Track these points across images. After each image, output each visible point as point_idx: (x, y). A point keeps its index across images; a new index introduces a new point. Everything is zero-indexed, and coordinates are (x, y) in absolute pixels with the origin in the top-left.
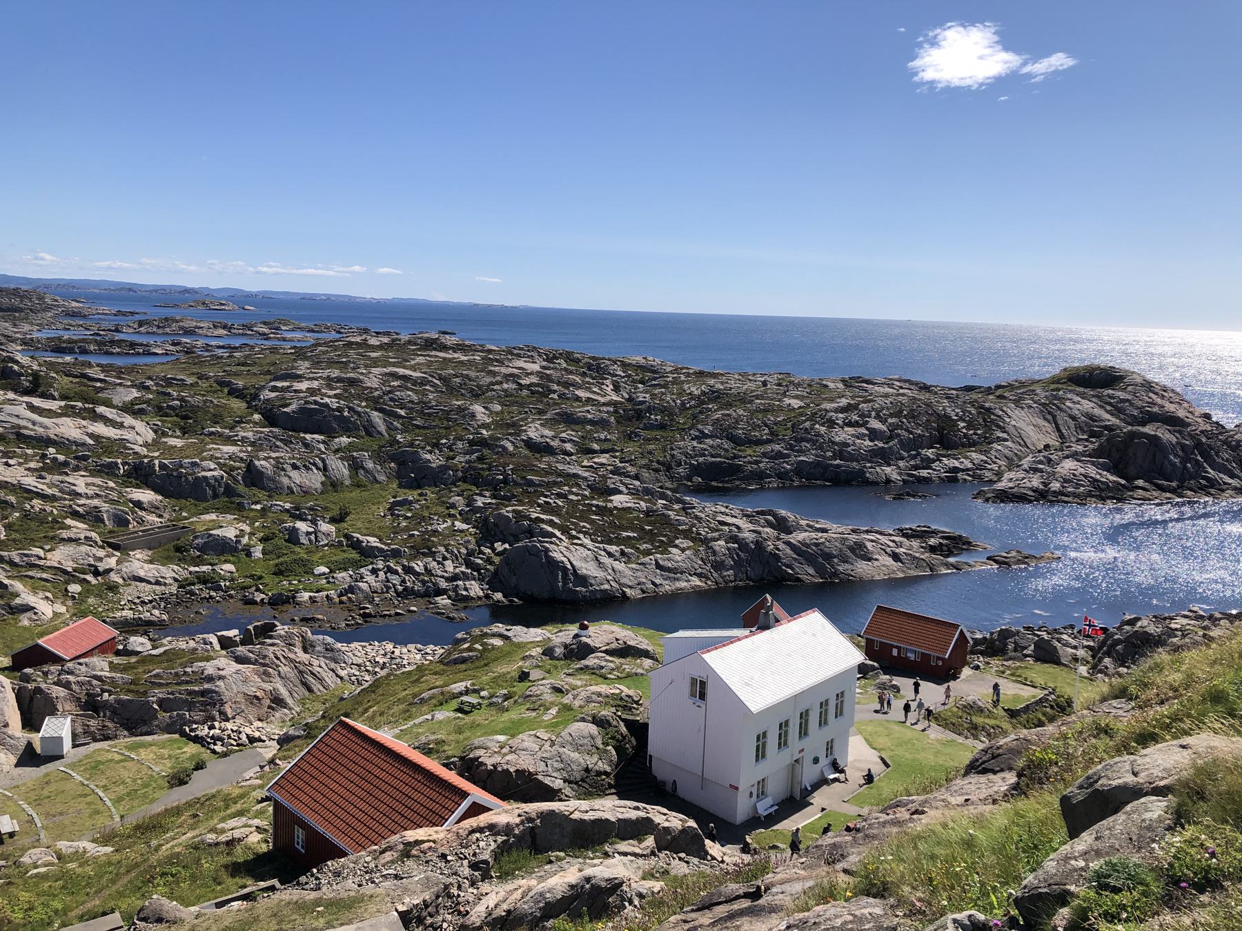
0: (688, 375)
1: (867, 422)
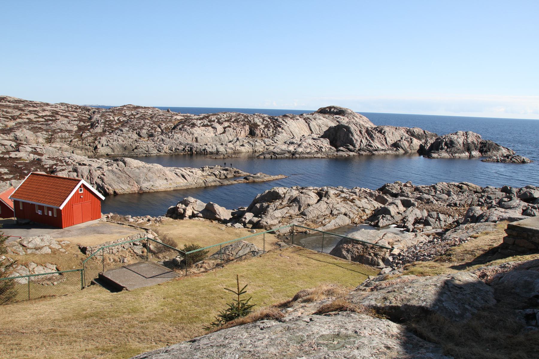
1: (212, 125)
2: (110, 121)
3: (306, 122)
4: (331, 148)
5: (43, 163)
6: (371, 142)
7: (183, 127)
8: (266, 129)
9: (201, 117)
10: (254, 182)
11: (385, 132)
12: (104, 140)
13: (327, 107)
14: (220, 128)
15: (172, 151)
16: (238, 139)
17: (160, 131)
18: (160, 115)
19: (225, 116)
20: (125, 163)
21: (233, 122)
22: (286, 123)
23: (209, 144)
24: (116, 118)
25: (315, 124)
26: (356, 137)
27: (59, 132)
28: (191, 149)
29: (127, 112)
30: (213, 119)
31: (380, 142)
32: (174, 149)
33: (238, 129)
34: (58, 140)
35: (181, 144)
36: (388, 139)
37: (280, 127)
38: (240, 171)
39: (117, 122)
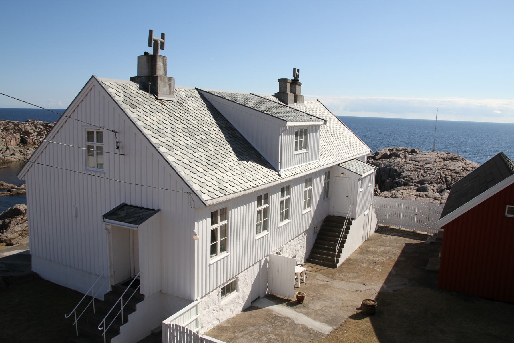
8: (39, 137)
10: (18, 194)
16: (7, 148)
33: (8, 138)
38: (5, 183)
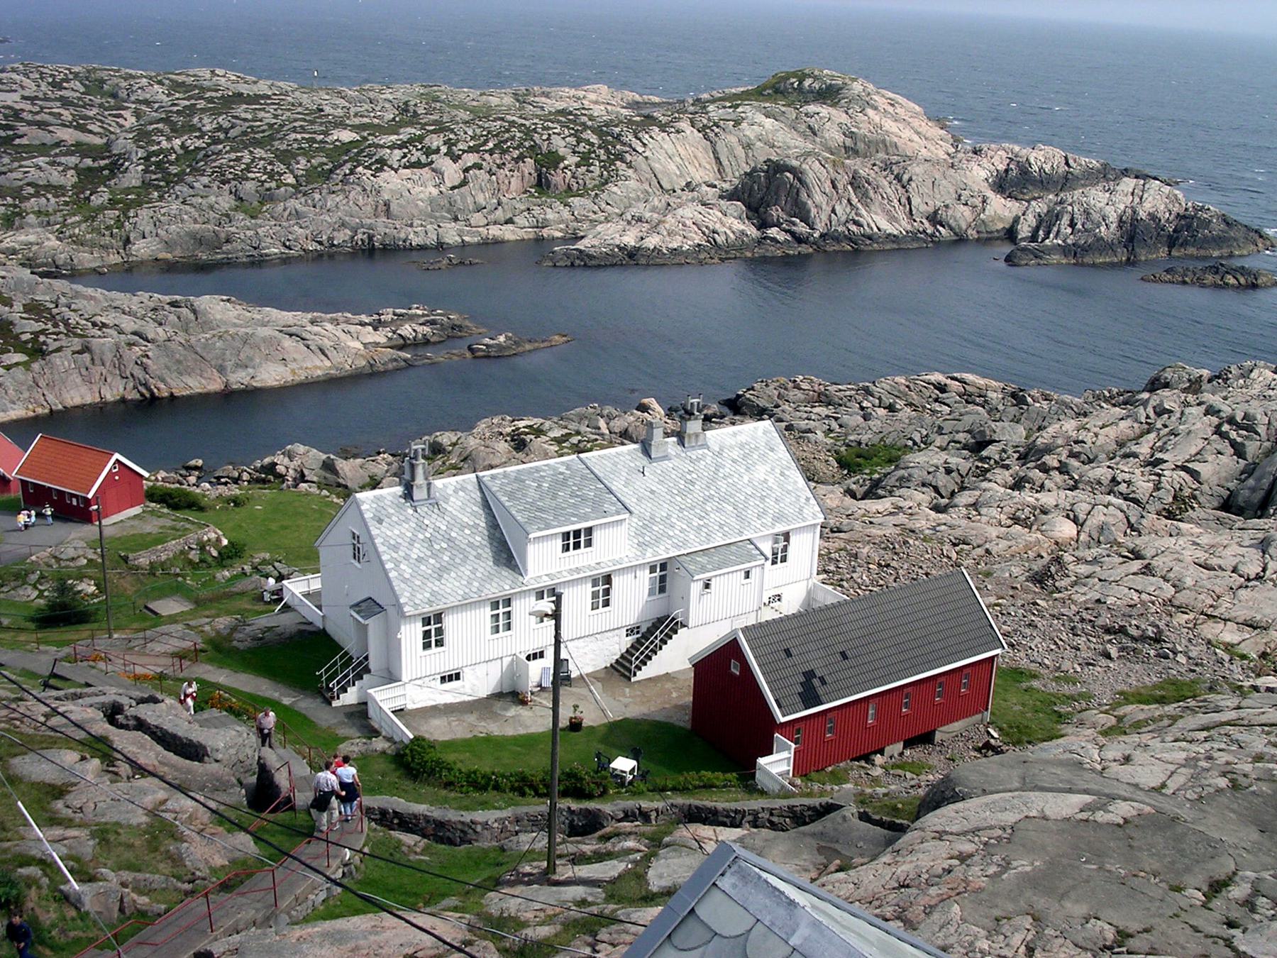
0: (211, 100)
2: (161, 151)
3: (706, 137)
4: (743, 232)
5: (17, 330)
6: (863, 212)
7: (352, 172)
8: (584, 169)
9: (404, 137)
11: (910, 179)
12: (145, 213)
13: (794, 75)
14: (452, 172)
15: (320, 243)
17: (291, 180)
18: (294, 130)
19: (470, 133)
20: (194, 312)
21: (491, 152)
22: (645, 145)
23: (417, 222)
24: (178, 142)
25: (733, 139)
26: (818, 197)
27: (32, 196)
28: (371, 238)
29: (206, 120)
30: (434, 146)
31: (888, 212)
32: (325, 237)
34: (31, 218)
35: (343, 225)
36: (916, 201)
37: (623, 160)
39: (181, 152)
